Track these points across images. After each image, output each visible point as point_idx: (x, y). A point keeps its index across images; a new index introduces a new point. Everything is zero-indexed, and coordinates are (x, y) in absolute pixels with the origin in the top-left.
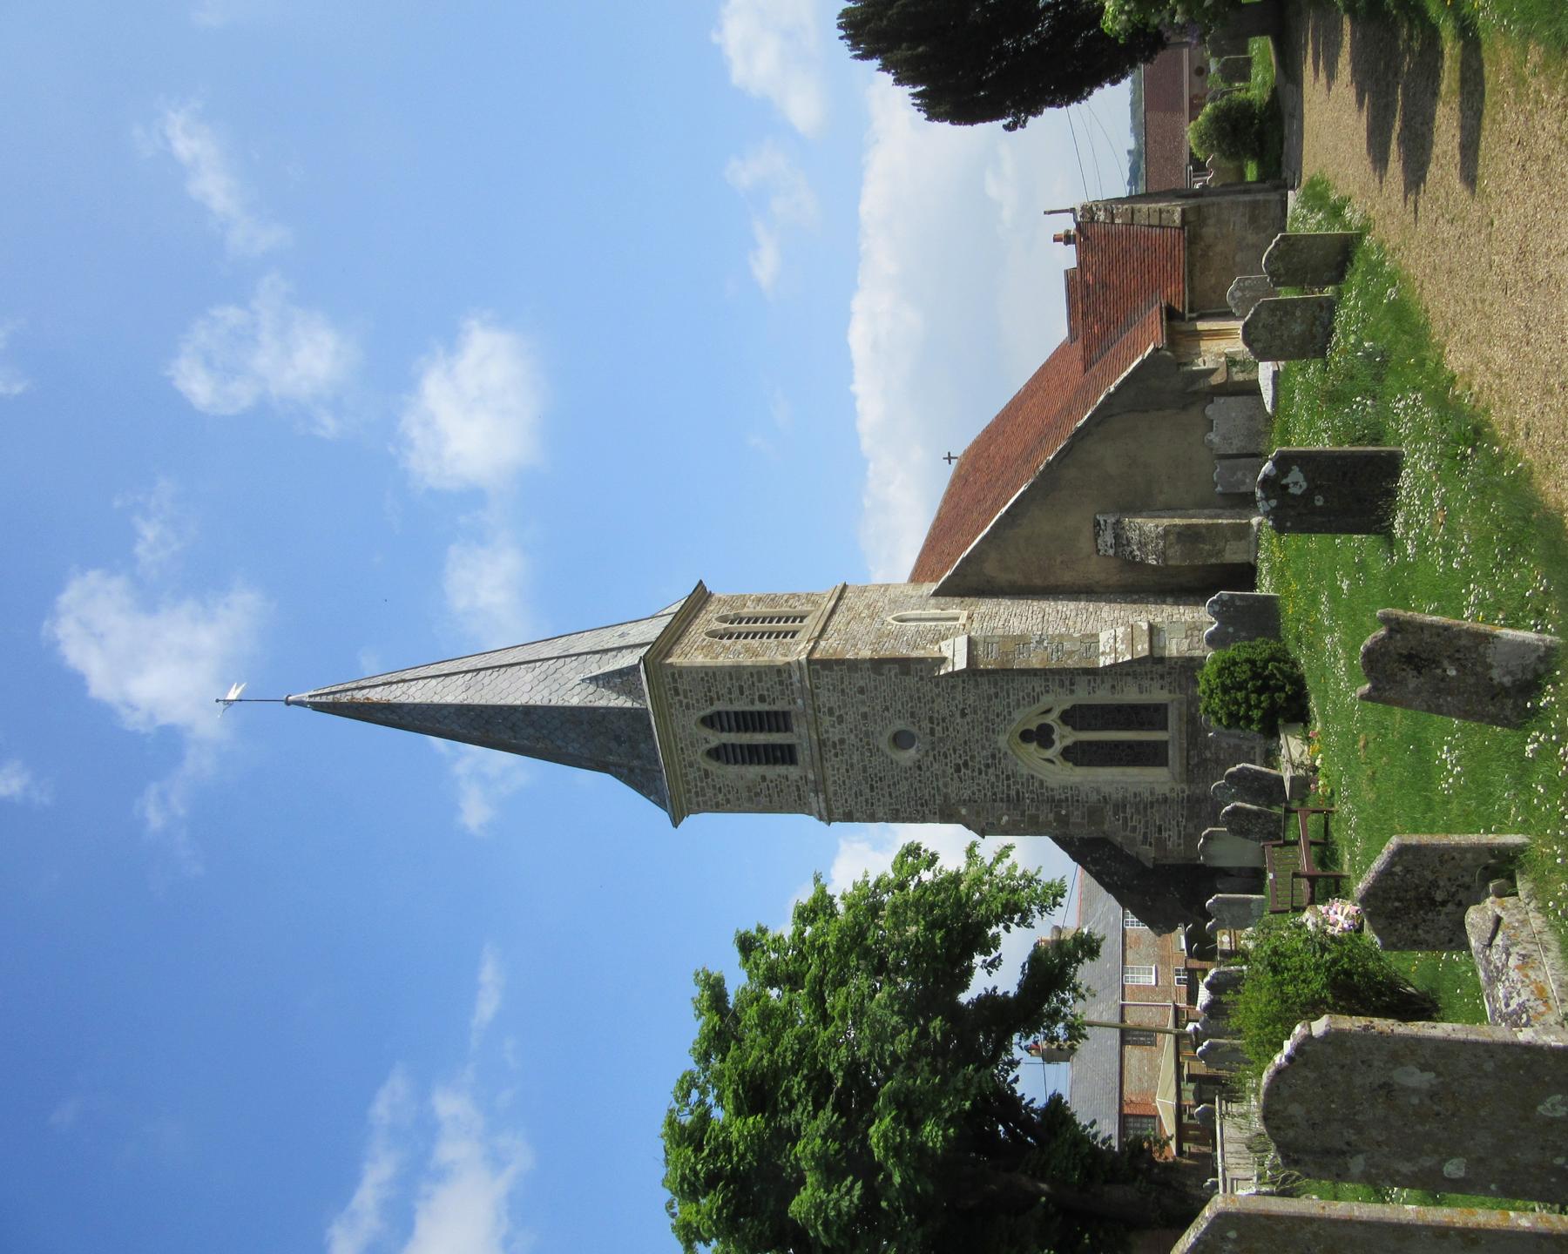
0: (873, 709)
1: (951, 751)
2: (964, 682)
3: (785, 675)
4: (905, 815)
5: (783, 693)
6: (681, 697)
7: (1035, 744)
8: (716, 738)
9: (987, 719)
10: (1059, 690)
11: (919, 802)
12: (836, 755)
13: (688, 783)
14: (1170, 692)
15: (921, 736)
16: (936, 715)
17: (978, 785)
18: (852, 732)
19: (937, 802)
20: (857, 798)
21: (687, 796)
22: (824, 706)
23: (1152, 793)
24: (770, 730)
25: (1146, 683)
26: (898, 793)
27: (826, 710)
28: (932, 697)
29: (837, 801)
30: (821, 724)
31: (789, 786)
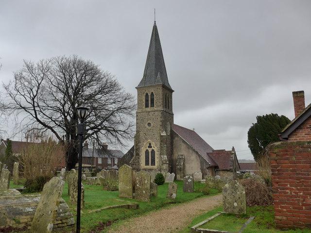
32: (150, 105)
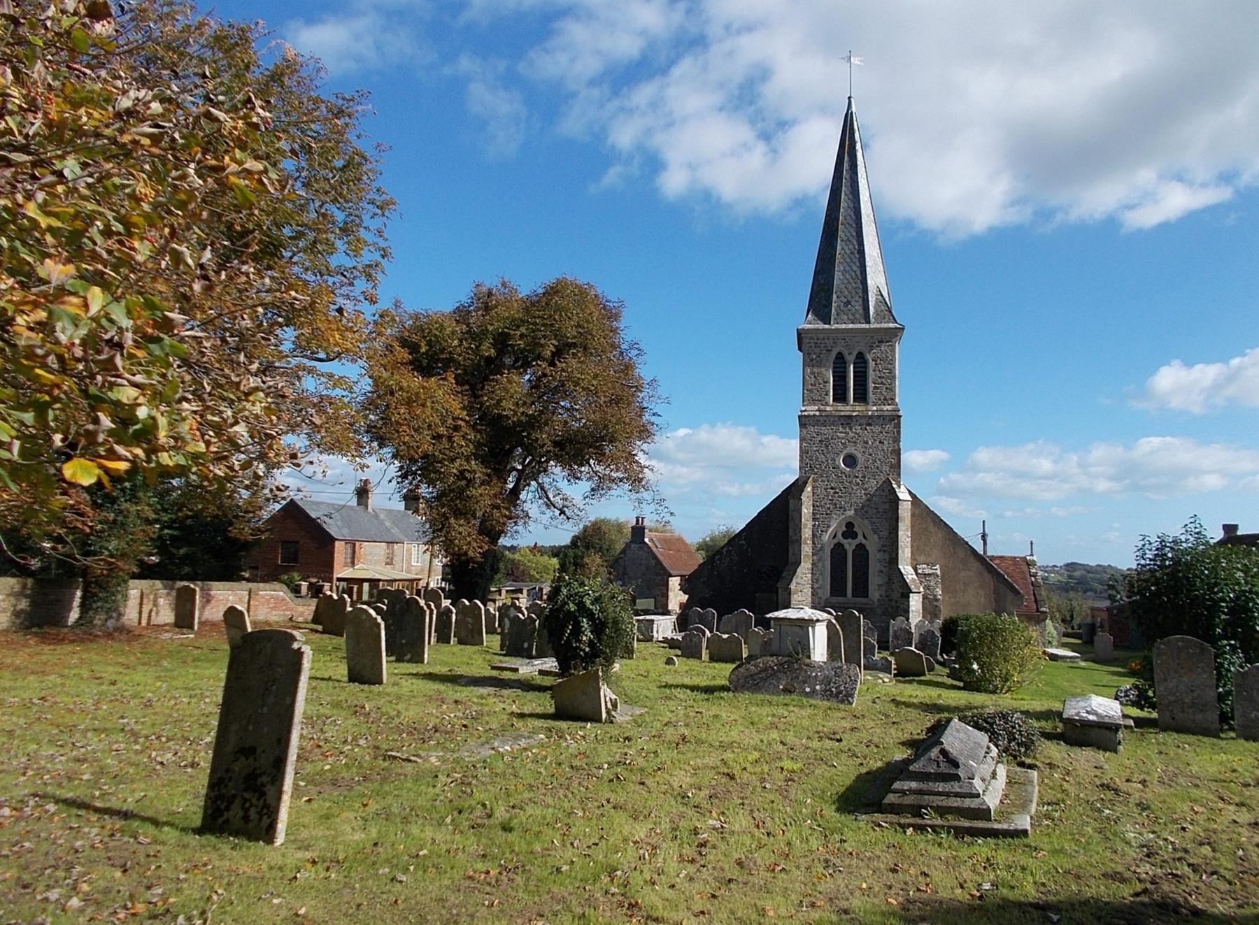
8: (851, 358)
25: (884, 588)
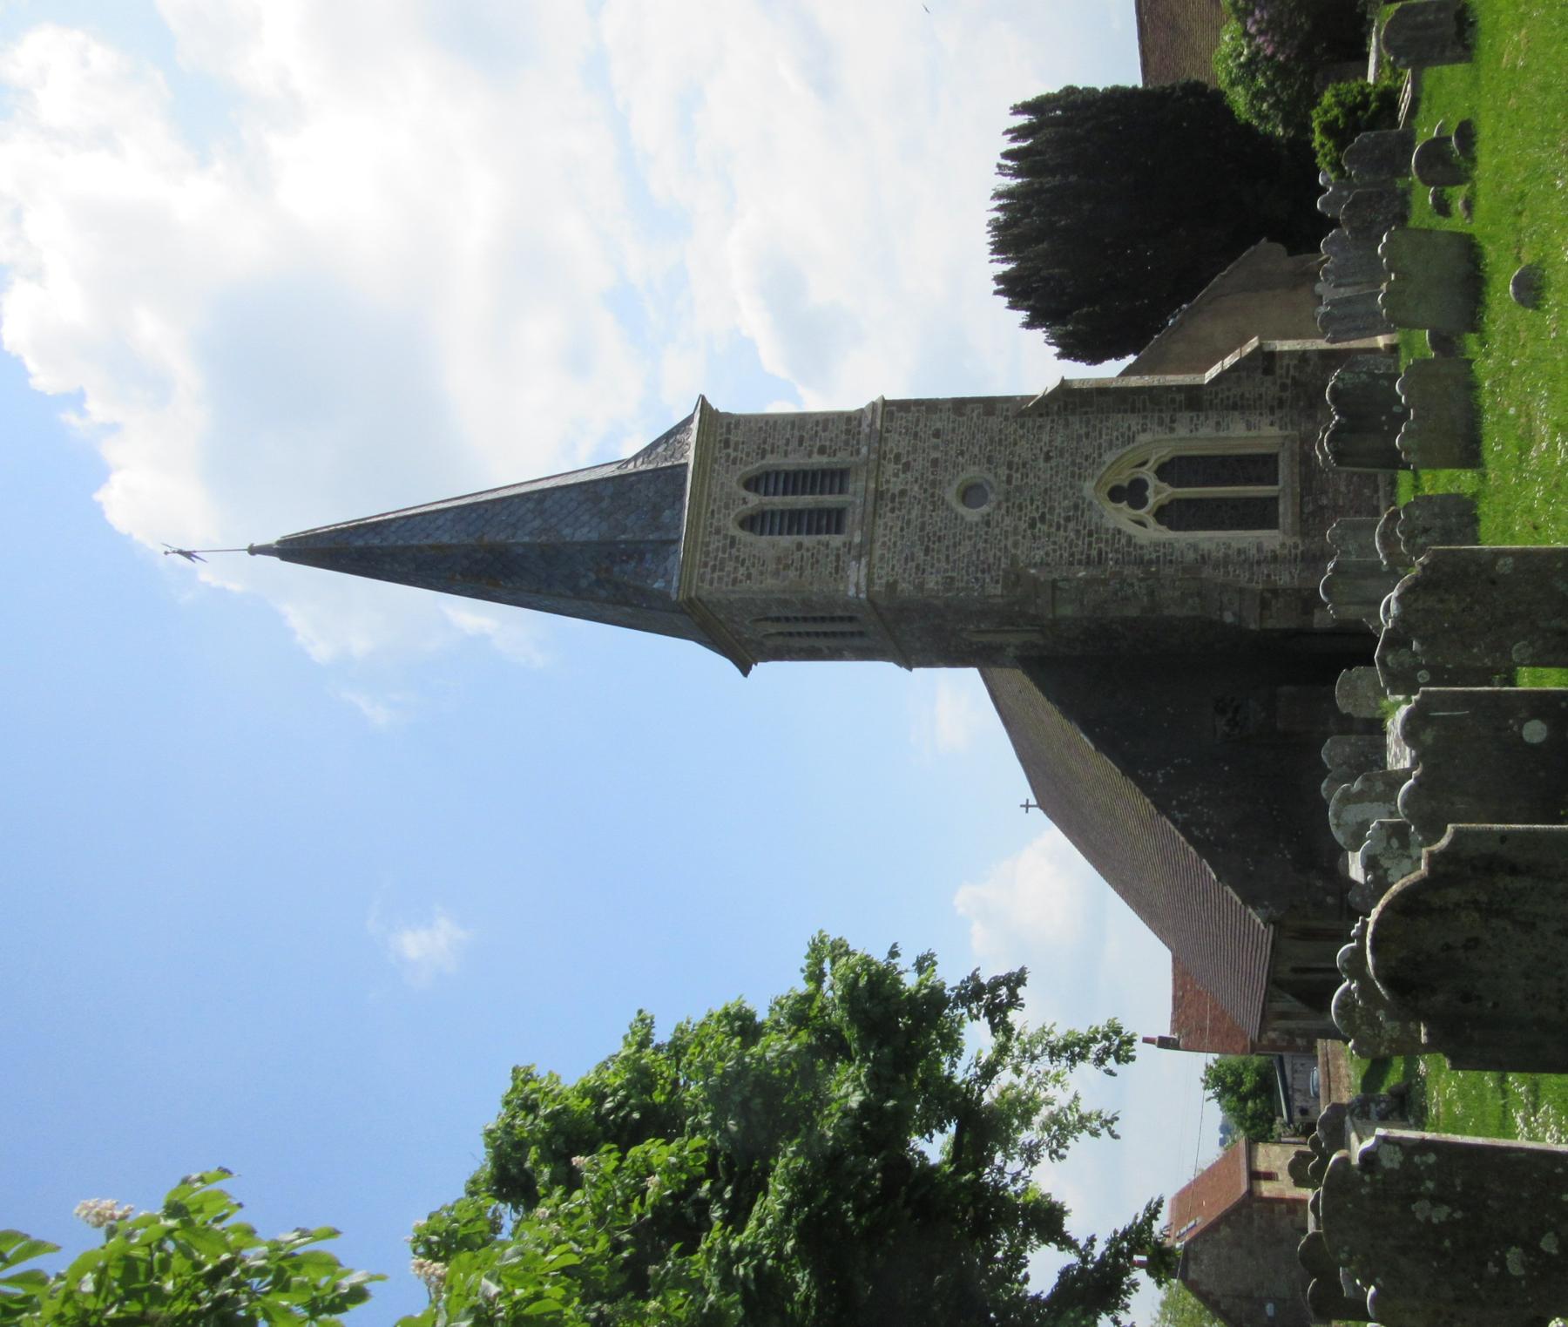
0: (946, 454)
1: (1028, 502)
2: (1053, 421)
3: (855, 423)
4: (963, 584)
5: (847, 443)
6: (730, 451)
7: (1125, 502)
9: (1073, 463)
10: (1159, 429)
11: (981, 567)
12: (892, 510)
13: (707, 554)
14: (1281, 428)
15: (995, 485)
16: (1016, 459)
17: (1055, 543)
18: (916, 481)
19: (1003, 566)
20: (906, 563)
21: (702, 570)
22: (891, 451)
23: (1259, 549)
24: (822, 493)
25: (1254, 419)
26: (956, 557)
27: (892, 456)
28: (1015, 439)
29: (882, 568)
30: (883, 473)
31: (827, 556)
32: (830, 500)
